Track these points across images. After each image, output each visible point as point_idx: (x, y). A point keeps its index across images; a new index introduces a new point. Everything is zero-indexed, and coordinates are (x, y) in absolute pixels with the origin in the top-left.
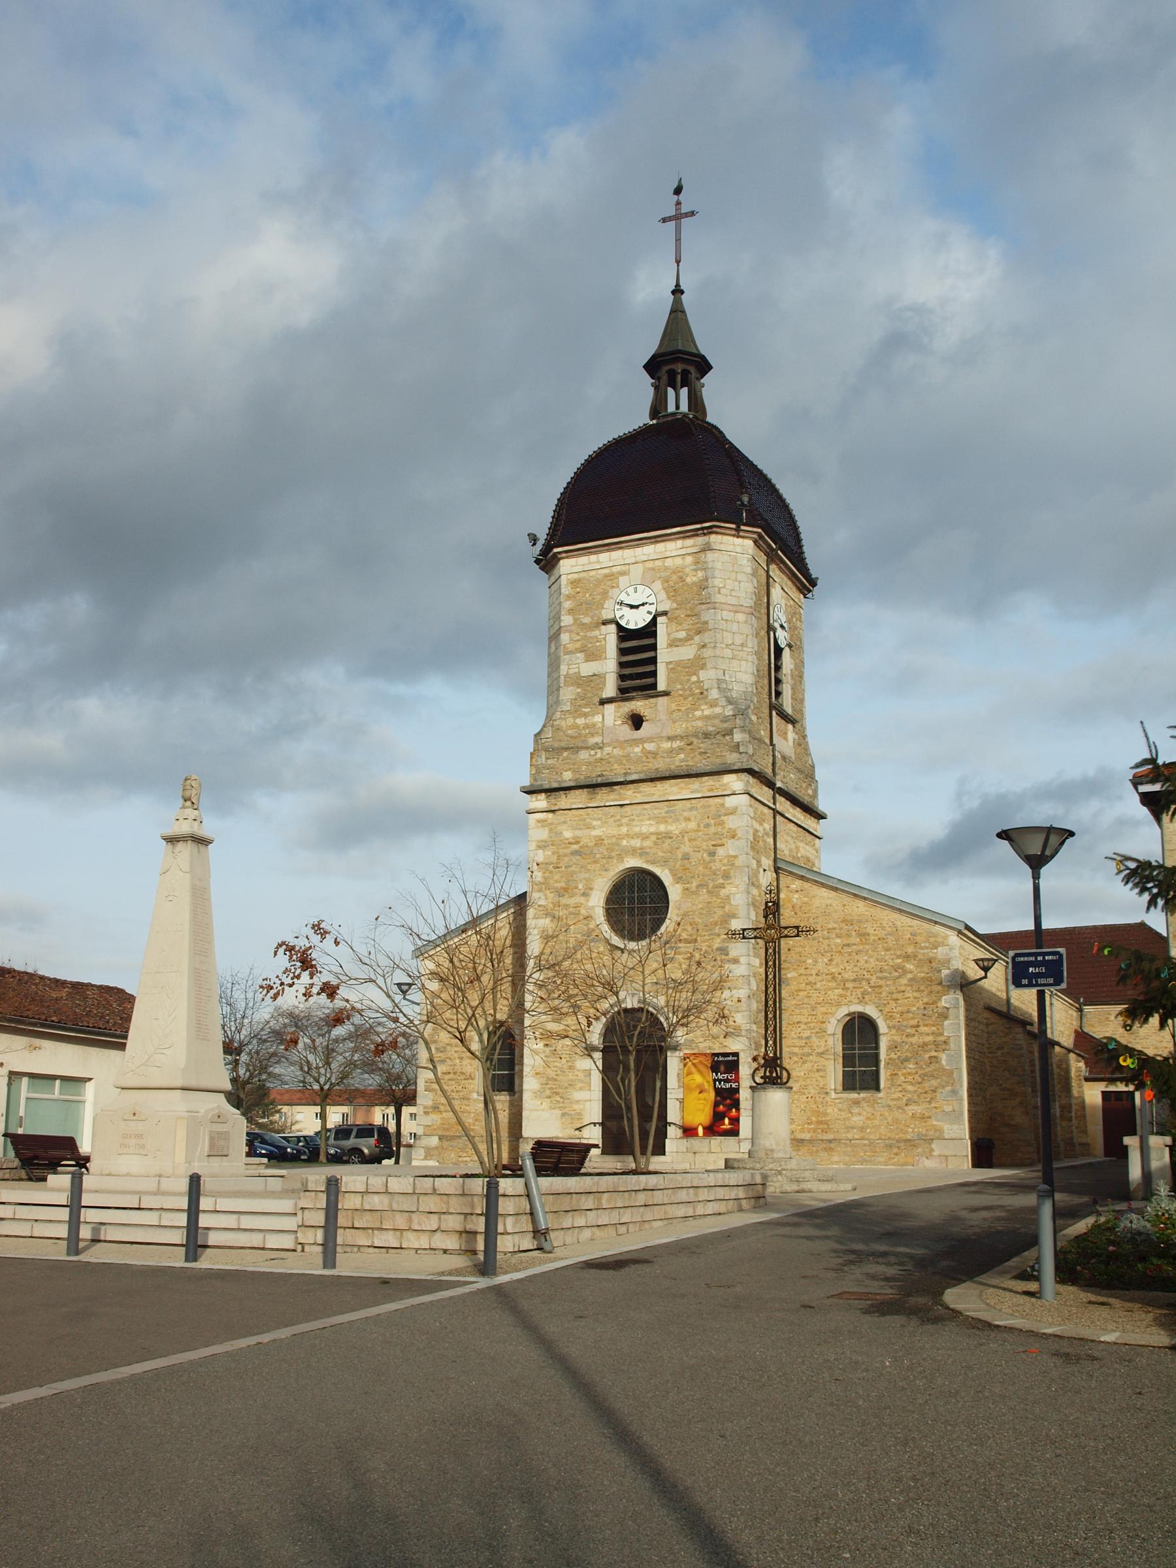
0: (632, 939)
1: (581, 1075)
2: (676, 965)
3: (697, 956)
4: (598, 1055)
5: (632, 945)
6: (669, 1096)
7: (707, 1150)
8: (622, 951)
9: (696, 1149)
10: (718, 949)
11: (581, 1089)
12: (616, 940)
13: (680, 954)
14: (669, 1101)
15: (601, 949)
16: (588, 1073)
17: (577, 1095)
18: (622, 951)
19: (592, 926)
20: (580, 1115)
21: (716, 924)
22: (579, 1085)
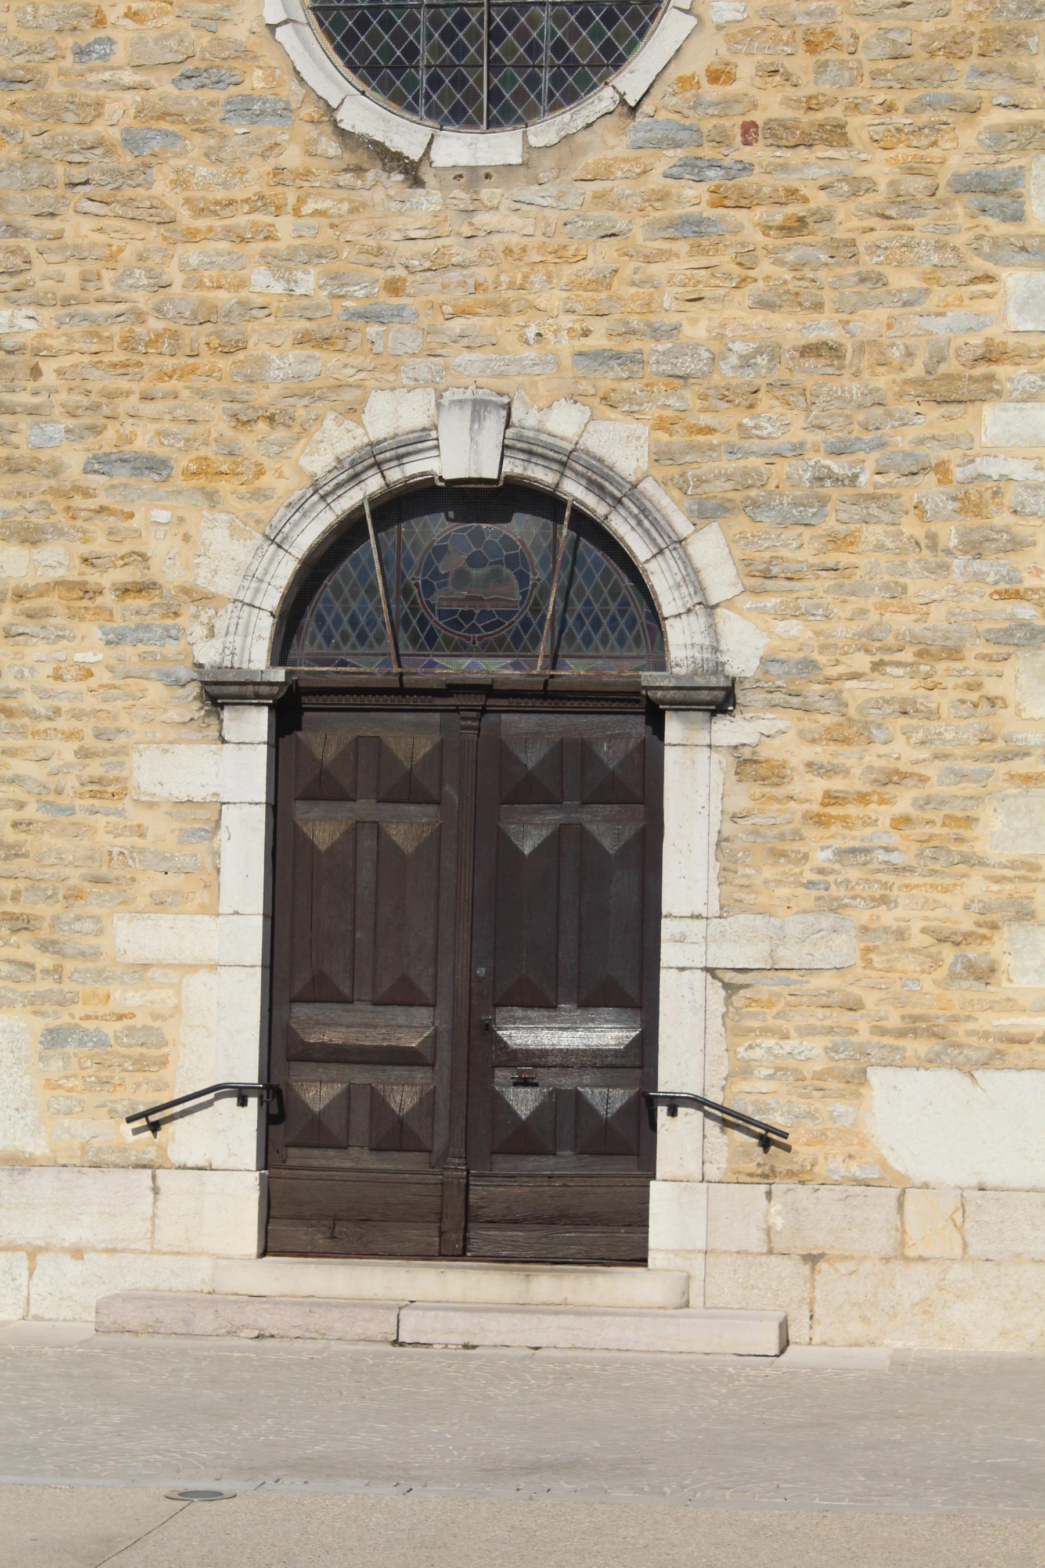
0: (459, 115)
1: (160, 828)
2: (725, 261)
3: (848, 219)
4: (255, 723)
5: (457, 148)
6: (669, 954)
7: (883, 1242)
8: (412, 172)
9: (818, 1241)
10: (963, 185)
11: (160, 904)
12: (367, 115)
13: (745, 202)
14: (667, 980)
15: (292, 157)
16: (206, 817)
17: (134, 936)
18: (412, 172)
19: (238, 32)
20: (150, 1049)
21: (953, 48)
22: (152, 882)
